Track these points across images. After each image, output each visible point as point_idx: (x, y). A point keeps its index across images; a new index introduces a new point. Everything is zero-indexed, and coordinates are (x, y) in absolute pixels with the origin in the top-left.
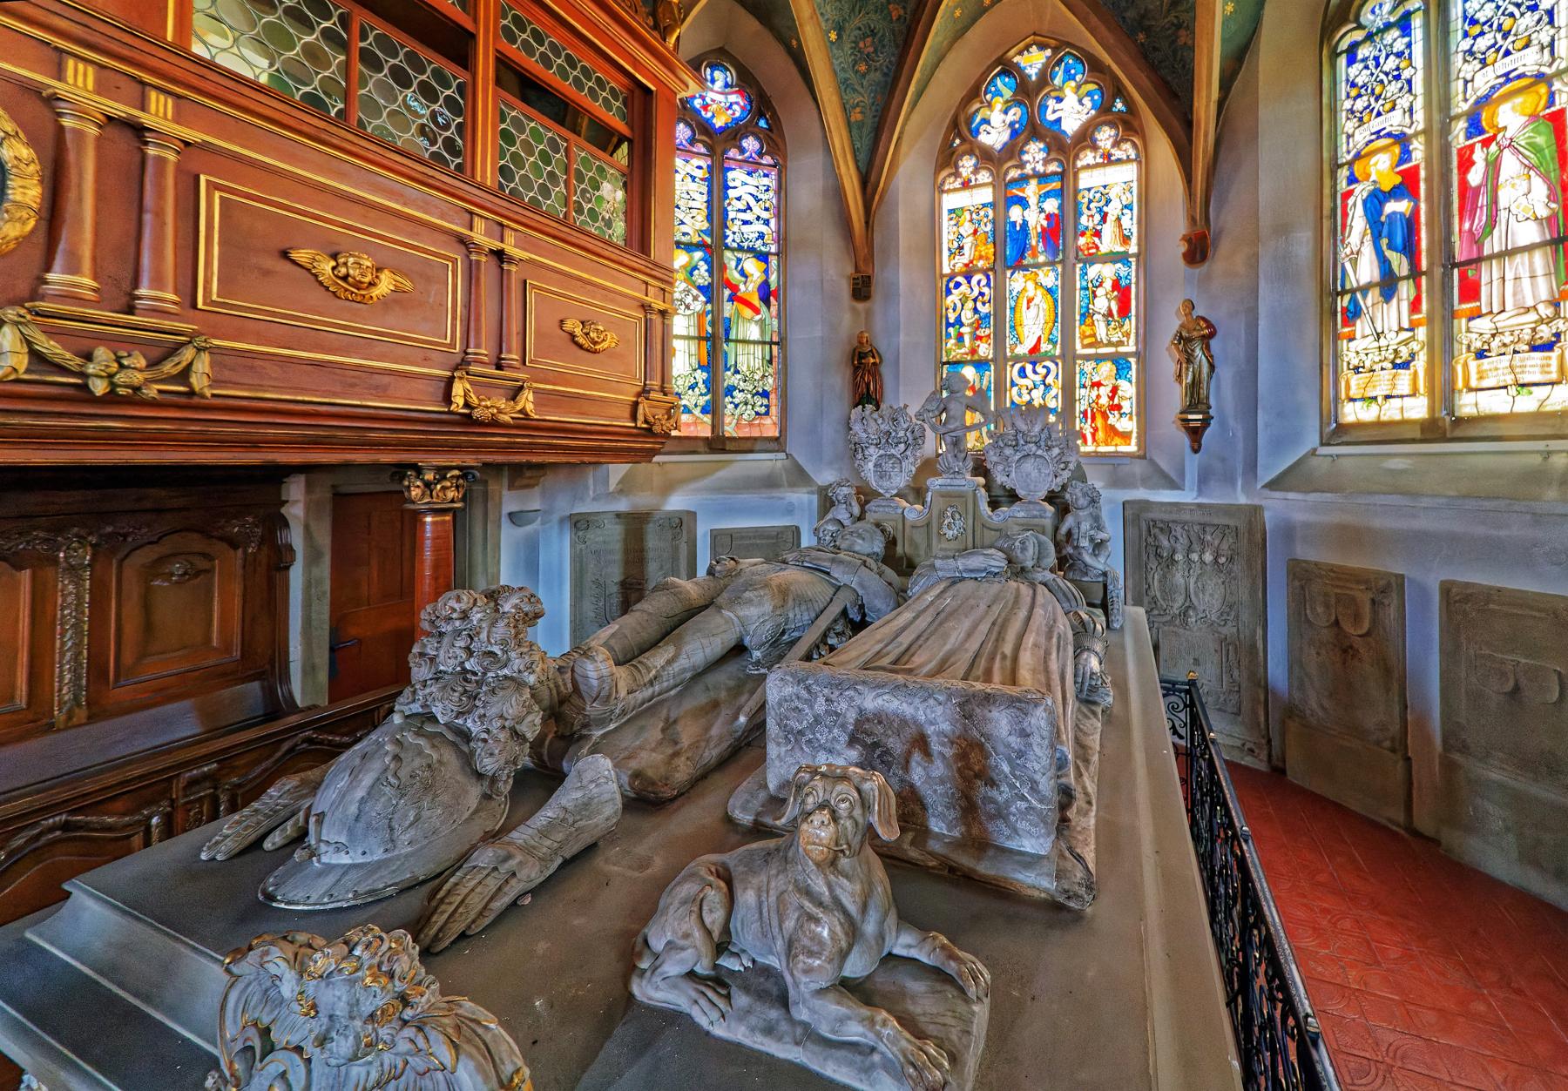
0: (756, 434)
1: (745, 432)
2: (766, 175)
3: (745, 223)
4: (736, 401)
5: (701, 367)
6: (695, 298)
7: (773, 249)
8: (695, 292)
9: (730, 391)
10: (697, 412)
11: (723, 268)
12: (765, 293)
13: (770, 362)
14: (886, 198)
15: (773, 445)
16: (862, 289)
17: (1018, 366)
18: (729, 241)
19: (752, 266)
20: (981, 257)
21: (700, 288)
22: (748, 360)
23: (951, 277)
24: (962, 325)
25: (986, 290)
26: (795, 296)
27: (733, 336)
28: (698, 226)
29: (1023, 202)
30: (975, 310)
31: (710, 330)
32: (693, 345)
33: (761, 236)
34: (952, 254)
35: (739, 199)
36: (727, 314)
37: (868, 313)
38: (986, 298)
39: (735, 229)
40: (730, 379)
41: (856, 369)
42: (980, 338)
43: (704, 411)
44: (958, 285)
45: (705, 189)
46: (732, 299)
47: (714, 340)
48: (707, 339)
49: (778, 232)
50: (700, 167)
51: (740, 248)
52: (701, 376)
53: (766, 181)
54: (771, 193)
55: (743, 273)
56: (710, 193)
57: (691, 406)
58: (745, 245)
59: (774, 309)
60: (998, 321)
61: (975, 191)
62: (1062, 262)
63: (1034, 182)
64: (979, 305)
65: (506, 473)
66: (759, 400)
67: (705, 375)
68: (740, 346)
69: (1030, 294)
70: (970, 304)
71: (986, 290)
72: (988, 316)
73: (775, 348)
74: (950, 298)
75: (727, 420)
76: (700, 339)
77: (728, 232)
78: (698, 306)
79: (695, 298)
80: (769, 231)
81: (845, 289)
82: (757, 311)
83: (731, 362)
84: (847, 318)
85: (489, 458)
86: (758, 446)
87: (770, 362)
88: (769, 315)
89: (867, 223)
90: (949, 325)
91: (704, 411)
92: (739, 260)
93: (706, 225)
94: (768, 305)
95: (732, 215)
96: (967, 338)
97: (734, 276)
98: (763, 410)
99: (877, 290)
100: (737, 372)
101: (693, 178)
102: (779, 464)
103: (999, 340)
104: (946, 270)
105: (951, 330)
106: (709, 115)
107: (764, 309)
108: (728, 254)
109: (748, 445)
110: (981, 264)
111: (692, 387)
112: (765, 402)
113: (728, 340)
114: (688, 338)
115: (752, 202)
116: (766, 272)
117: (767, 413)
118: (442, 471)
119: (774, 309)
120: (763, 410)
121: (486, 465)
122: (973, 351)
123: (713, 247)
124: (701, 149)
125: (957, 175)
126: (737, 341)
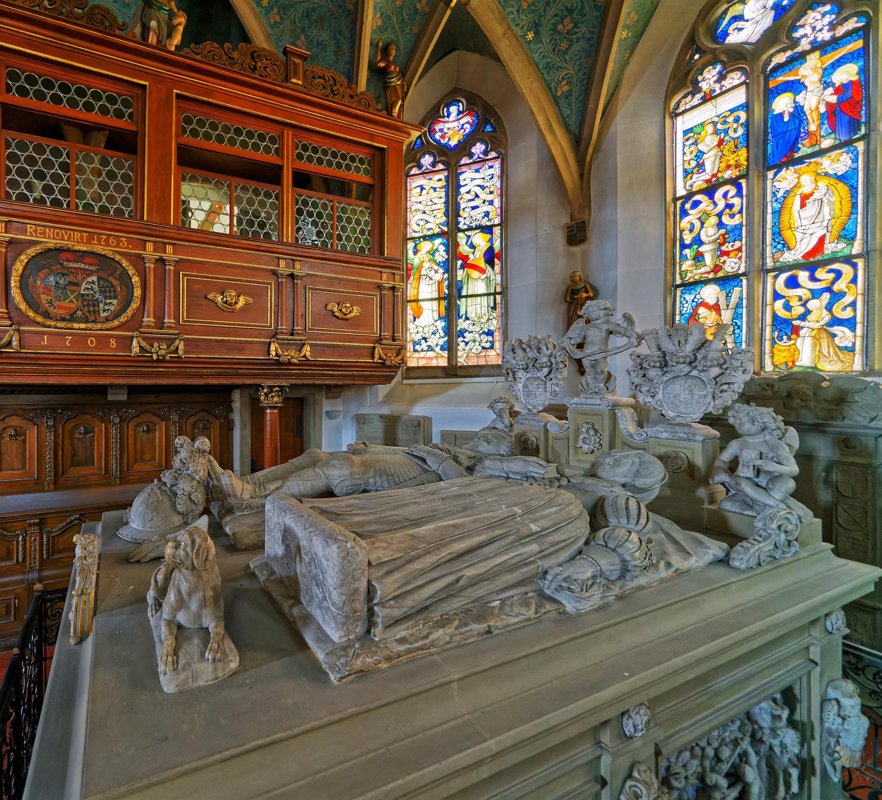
0: (482, 362)
1: (473, 362)
2: (491, 167)
3: (474, 208)
4: (466, 340)
5: (440, 318)
6: (436, 272)
7: (497, 221)
8: (436, 267)
9: (462, 333)
10: (438, 349)
11: (457, 245)
12: (490, 257)
13: (494, 308)
14: (604, 145)
15: (496, 371)
16: (576, 234)
17: (784, 276)
18: (461, 226)
19: (481, 240)
20: (728, 167)
21: (438, 264)
22: (476, 310)
23: (690, 195)
24: (701, 243)
25: (736, 201)
26: (514, 254)
27: (464, 293)
28: (438, 221)
29: (796, 87)
30: (720, 225)
31: (447, 291)
32: (435, 303)
33: (487, 214)
34: (686, 173)
35: (468, 192)
36: (459, 278)
37: (585, 254)
38: (736, 209)
39: (465, 215)
40: (462, 324)
41: (570, 304)
42: (727, 253)
43: (442, 349)
44: (696, 204)
45: (443, 194)
46: (463, 267)
47: (451, 298)
48: (444, 299)
49: (501, 208)
50: (440, 180)
51: (470, 229)
52: (441, 324)
53: (491, 171)
54: (495, 179)
55: (472, 246)
56: (447, 195)
57: (433, 346)
58: (473, 225)
59: (497, 268)
60: (759, 229)
61: (719, 100)
62: (866, 137)
63: (813, 60)
64: (726, 219)
65: (324, 390)
66: (485, 338)
67: (443, 324)
68: (470, 300)
69: (806, 190)
70: (714, 220)
71: (736, 201)
72: (739, 227)
73: (498, 297)
74: (686, 220)
75: (460, 354)
76: (439, 299)
77: (460, 219)
78: (438, 277)
79: (436, 272)
80: (494, 211)
81: (560, 238)
82: (483, 271)
83: (463, 312)
84: (562, 262)
85: (294, 382)
86: (483, 372)
87: (494, 308)
88: (495, 275)
89: (581, 175)
90: (684, 246)
91: (442, 349)
92: (469, 237)
93: (444, 219)
94: (492, 265)
95: (462, 206)
96: (708, 258)
97: (464, 249)
98: (488, 345)
99: (593, 235)
100: (467, 318)
101: (435, 189)
102: (499, 385)
103: (756, 250)
104: (681, 192)
105: (687, 251)
106: (446, 140)
107: (489, 269)
108: (460, 235)
109: (476, 371)
110: (728, 174)
111: (434, 333)
112: (490, 338)
113: (460, 297)
114: (432, 299)
115: (479, 190)
116: (491, 240)
117: (492, 347)
118: (271, 388)
119: (497, 268)
120: (488, 345)
121: (292, 385)
122: (717, 268)
123: (451, 232)
124: (441, 166)
125: (696, 89)
126: (467, 296)
